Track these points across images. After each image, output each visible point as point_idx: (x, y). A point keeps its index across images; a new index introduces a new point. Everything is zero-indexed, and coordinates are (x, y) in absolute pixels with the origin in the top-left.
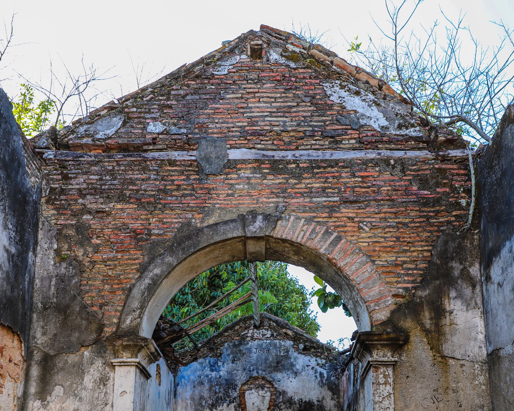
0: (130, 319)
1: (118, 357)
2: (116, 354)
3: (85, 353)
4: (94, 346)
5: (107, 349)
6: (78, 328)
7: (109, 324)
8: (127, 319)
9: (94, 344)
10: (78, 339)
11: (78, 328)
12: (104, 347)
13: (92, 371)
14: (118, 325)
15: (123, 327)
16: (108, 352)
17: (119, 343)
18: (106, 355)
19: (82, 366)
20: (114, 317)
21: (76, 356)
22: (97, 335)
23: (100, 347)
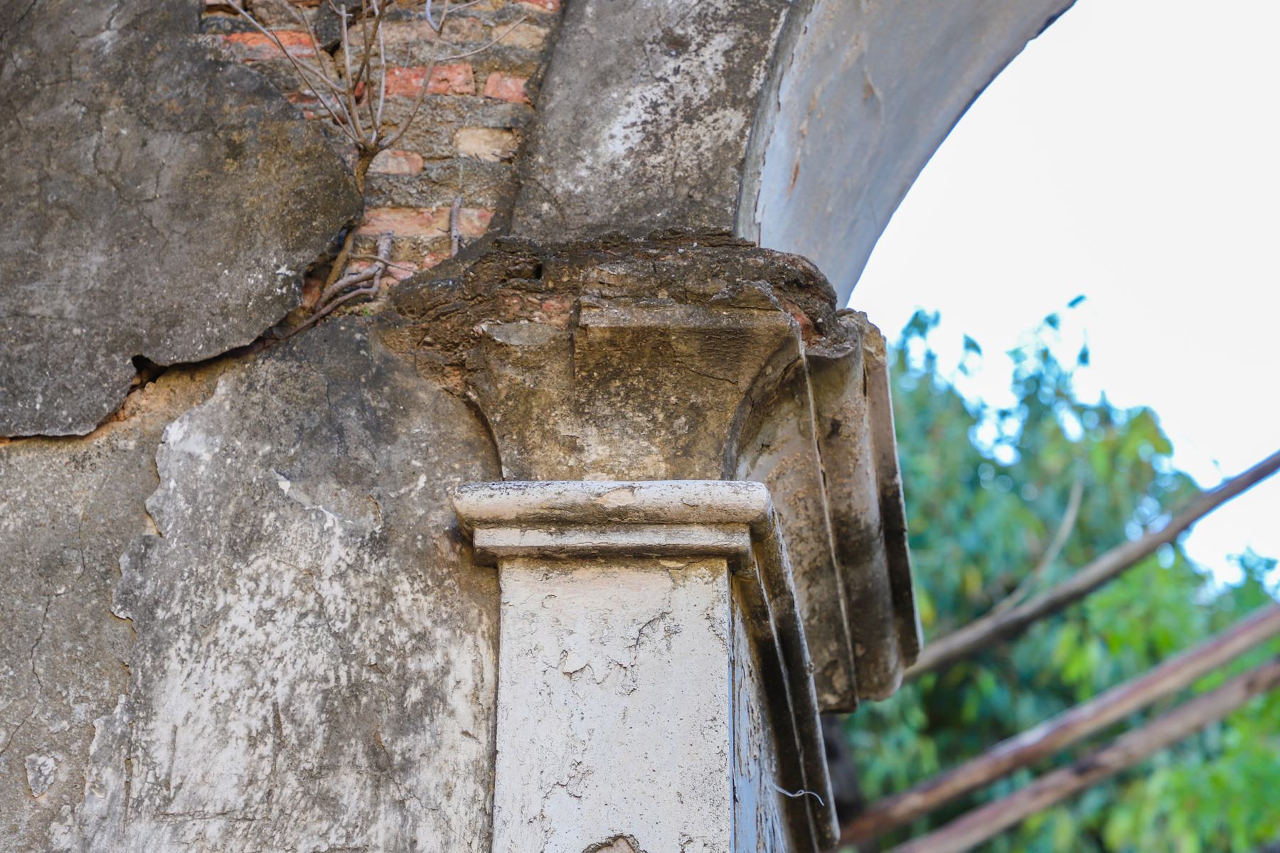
0: (637, 113)
1: (524, 474)
2: (493, 440)
3: (175, 432)
4: (266, 369)
5: (402, 403)
6: (113, 201)
7: (422, 175)
8: (607, 116)
9: (265, 343)
10: (107, 298)
11: (113, 201)
12: (377, 381)
13: (242, 612)
14: (515, 182)
15: (563, 184)
16: (419, 425)
17: (533, 326)
18: (396, 454)
19: (139, 560)
20: (470, 108)
21: (79, 463)
22: (307, 256)
23: (334, 381)
